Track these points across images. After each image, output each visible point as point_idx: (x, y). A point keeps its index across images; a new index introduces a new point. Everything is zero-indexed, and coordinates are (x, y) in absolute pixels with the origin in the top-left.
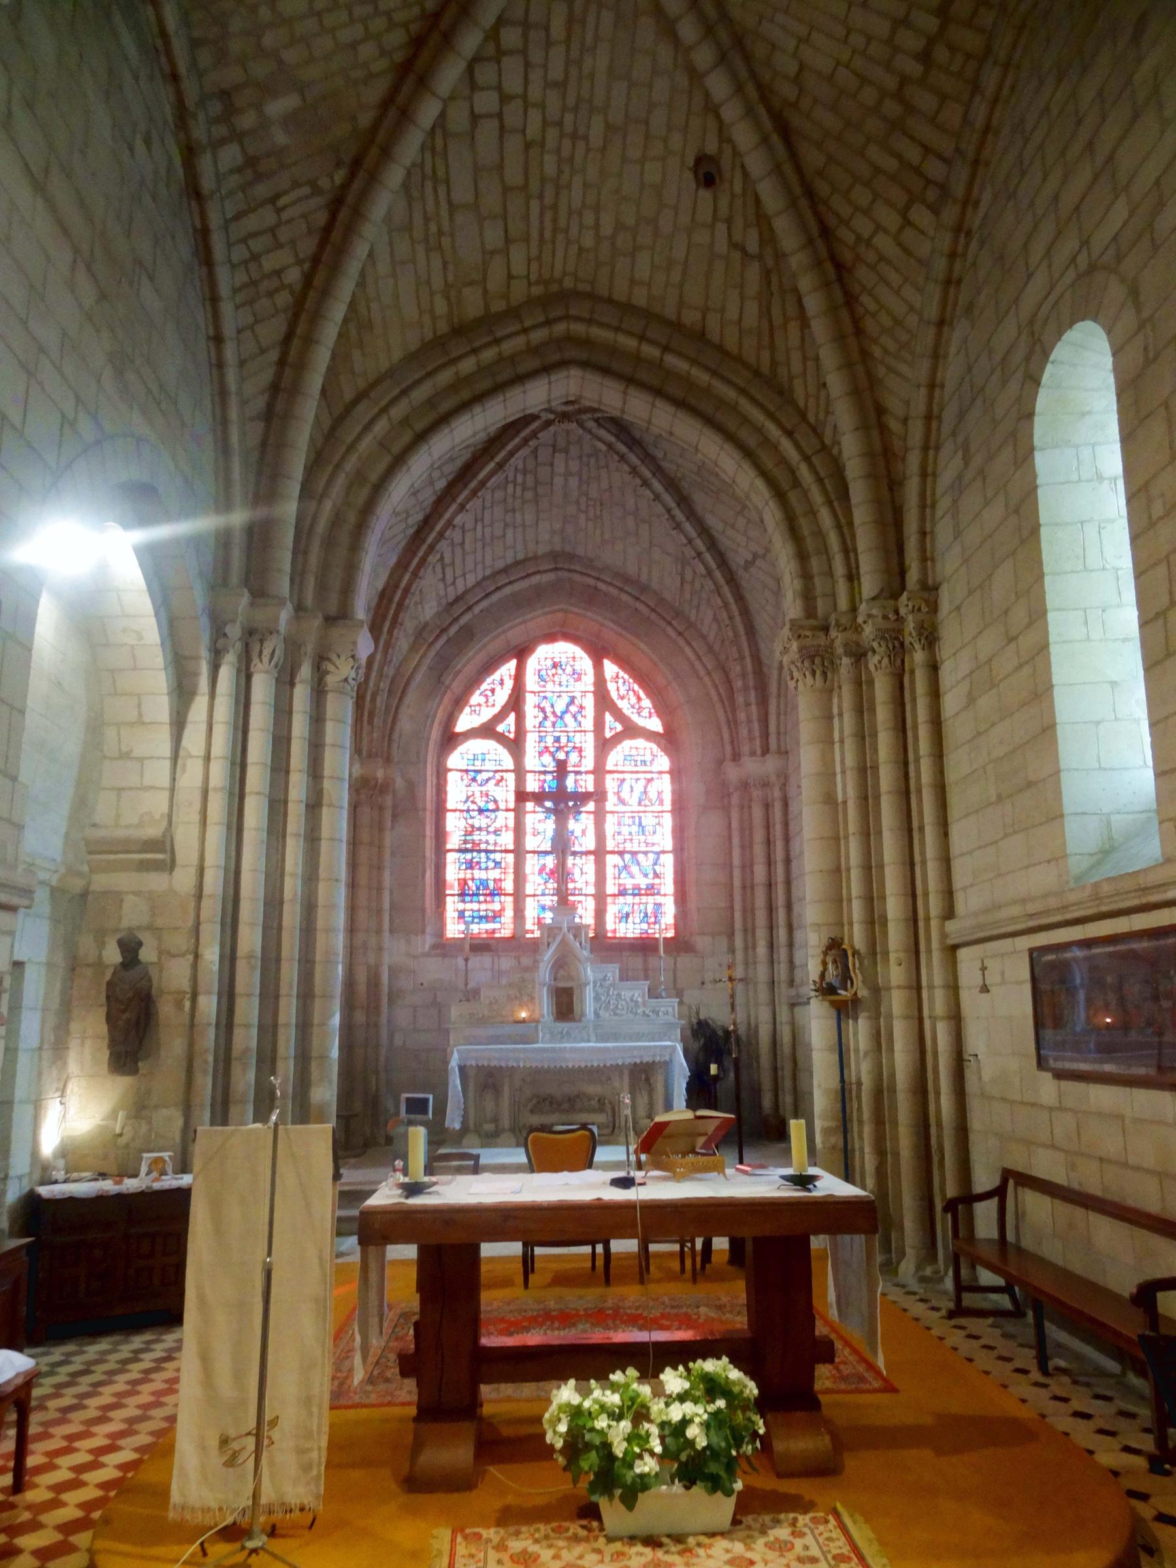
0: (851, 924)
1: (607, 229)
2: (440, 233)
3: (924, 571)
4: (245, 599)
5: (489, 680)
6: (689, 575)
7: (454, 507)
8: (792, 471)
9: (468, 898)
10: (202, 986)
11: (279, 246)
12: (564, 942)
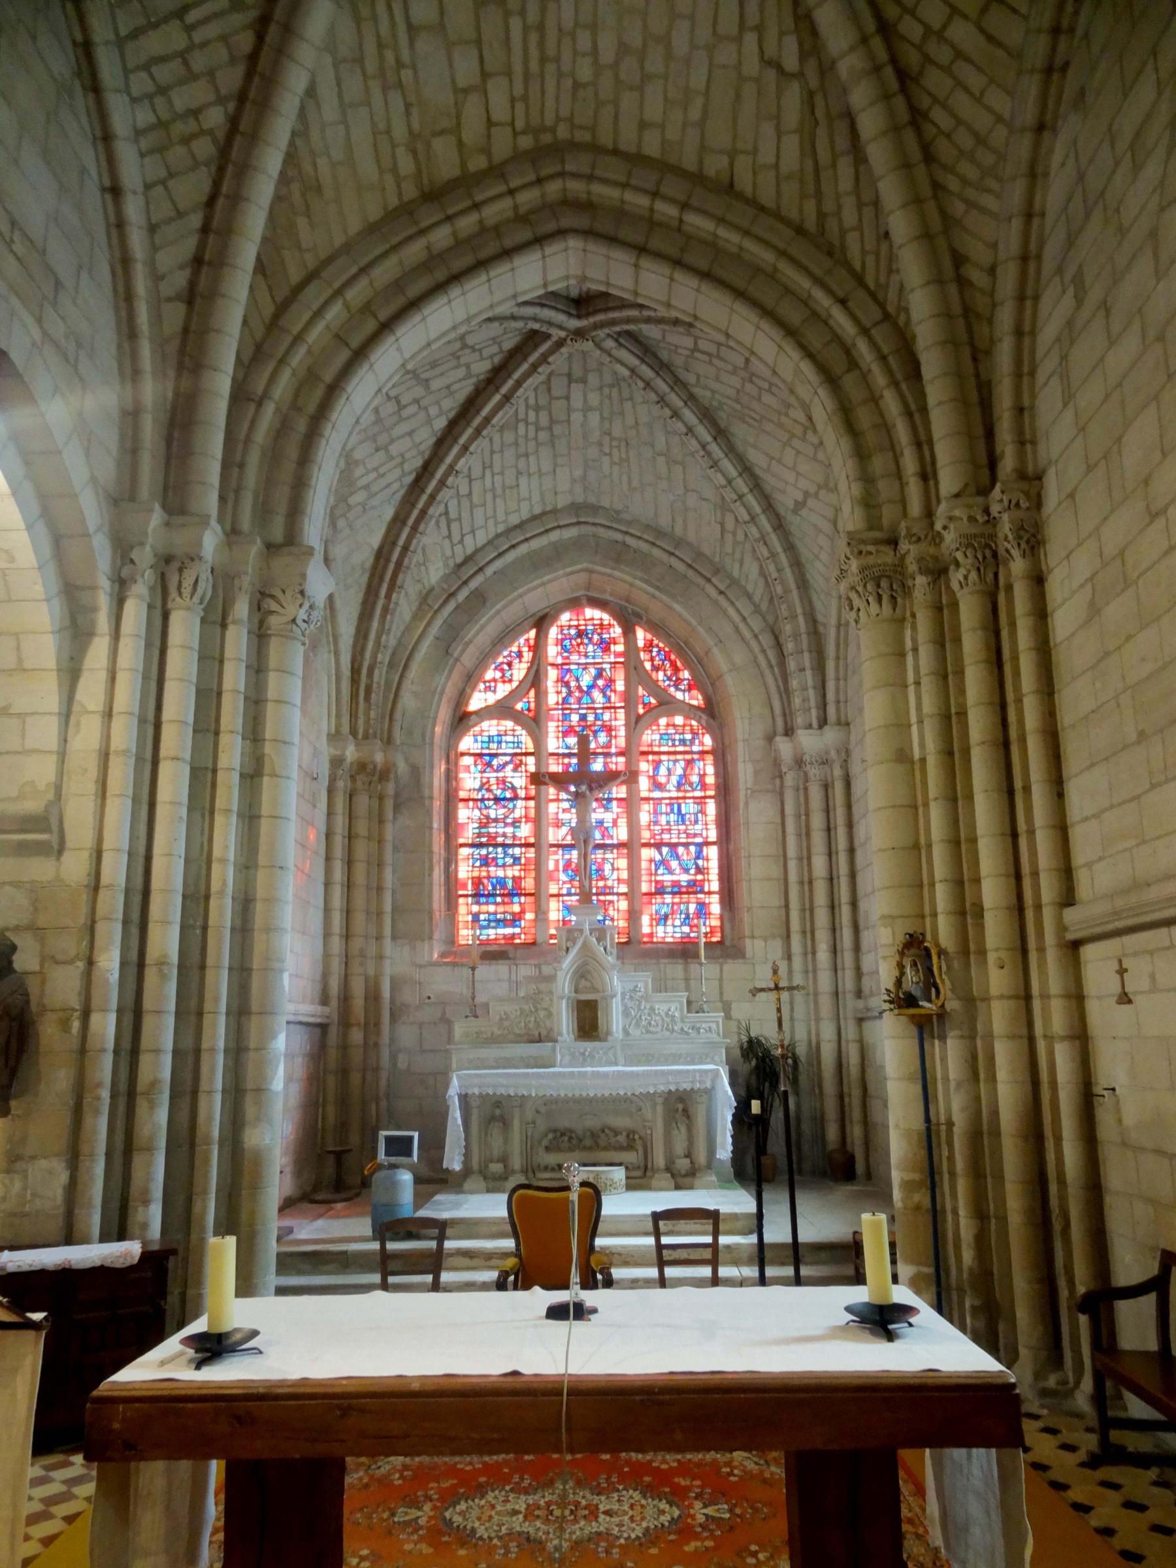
0: (934, 915)
1: (607, 55)
2: (399, 64)
3: (1021, 456)
4: (157, 517)
5: (506, 653)
6: (730, 525)
7: (455, 450)
8: (848, 351)
9: (483, 900)
10: (95, 1002)
11: (191, 77)
12: (585, 946)
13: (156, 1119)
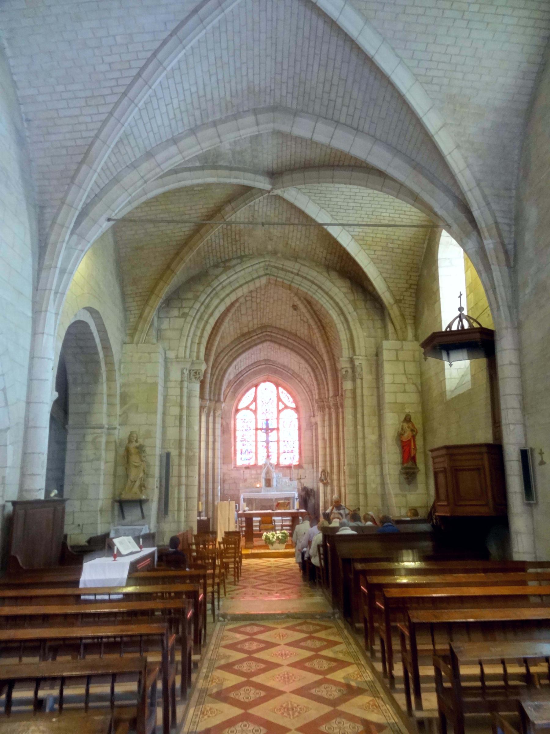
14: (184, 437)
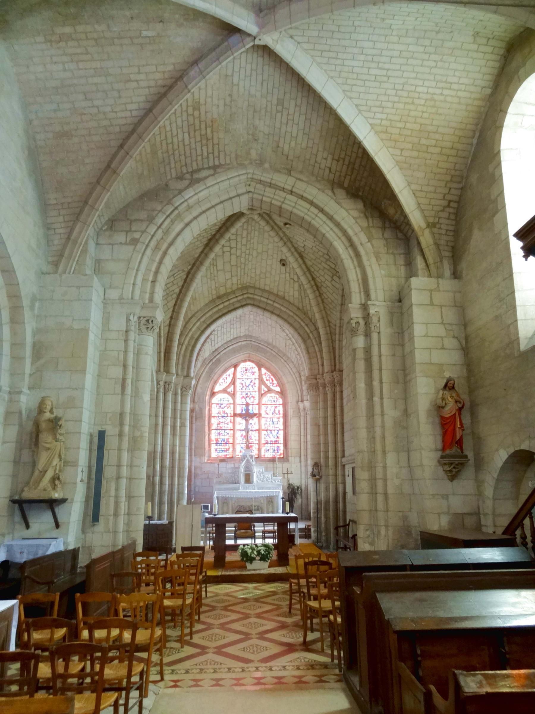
8: (308, 335)
11: (174, 285)
12: (248, 460)
13: (166, 498)
14: (128, 409)
